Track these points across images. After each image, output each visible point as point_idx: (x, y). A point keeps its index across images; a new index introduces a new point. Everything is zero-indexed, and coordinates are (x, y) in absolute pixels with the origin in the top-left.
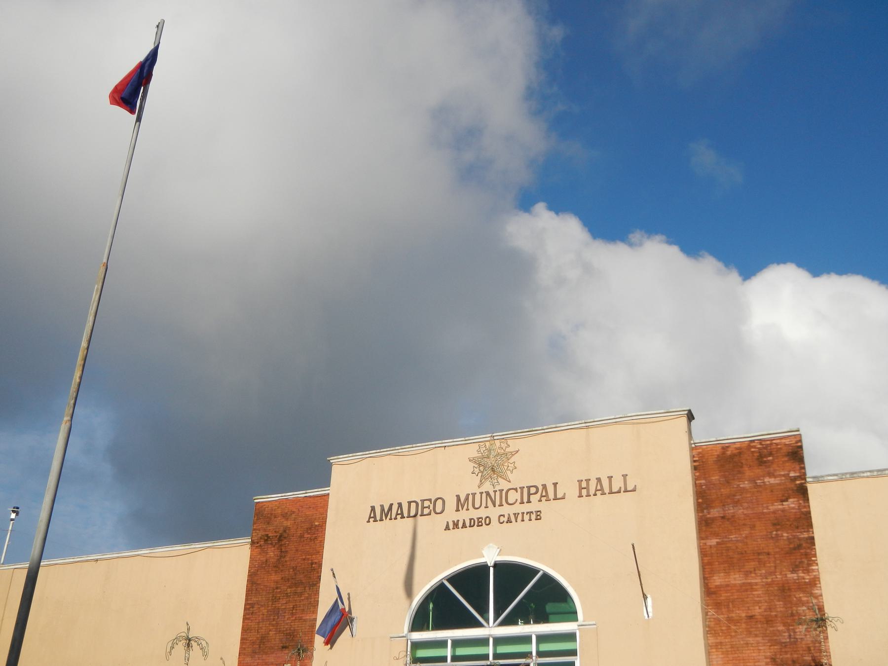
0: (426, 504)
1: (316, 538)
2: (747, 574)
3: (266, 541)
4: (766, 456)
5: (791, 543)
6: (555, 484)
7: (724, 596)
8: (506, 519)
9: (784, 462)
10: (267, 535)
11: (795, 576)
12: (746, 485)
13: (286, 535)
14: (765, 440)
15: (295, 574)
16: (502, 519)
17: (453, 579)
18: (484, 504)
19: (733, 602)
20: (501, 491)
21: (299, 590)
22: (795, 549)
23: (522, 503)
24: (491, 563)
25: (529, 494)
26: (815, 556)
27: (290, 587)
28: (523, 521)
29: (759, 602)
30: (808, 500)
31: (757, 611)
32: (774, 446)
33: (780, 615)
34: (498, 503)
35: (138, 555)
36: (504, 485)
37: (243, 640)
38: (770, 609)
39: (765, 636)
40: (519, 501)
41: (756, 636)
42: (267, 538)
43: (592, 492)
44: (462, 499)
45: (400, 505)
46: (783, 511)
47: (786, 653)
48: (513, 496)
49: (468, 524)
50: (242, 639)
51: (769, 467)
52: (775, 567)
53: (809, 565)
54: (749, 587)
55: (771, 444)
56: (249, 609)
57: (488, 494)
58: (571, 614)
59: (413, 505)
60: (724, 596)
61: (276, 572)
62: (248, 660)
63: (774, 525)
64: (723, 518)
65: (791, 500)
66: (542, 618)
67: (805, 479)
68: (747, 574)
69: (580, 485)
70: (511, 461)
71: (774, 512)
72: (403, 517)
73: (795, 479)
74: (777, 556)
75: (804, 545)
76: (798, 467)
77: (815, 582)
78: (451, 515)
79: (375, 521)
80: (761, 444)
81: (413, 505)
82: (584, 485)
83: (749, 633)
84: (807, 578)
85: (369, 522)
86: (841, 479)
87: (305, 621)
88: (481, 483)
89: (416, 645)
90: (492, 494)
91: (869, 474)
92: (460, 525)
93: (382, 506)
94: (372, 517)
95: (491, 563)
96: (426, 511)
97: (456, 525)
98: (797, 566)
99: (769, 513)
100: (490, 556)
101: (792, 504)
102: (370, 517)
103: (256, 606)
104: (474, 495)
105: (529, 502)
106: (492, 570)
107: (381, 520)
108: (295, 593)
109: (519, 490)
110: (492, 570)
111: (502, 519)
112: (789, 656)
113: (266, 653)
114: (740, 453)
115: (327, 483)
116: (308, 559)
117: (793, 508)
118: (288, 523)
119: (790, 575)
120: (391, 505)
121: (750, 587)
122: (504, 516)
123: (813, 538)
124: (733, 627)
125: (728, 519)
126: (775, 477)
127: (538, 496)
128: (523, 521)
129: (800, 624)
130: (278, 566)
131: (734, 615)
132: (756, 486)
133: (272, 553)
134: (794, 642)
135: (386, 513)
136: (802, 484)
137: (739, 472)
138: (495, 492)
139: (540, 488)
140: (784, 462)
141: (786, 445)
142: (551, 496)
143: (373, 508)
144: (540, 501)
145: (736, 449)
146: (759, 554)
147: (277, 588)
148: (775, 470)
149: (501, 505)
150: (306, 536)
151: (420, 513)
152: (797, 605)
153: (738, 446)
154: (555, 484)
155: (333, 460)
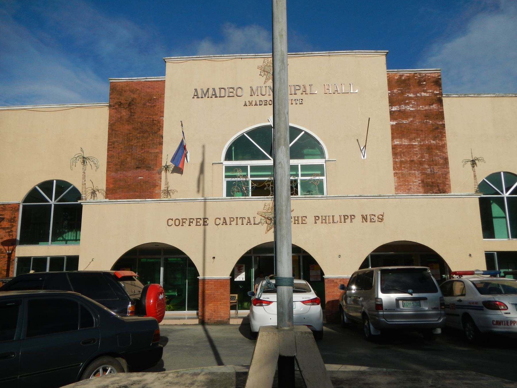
0: (231, 90)
1: (155, 106)
2: (411, 140)
3: (120, 105)
5: (433, 126)
7: (399, 150)
9: (432, 86)
10: (120, 102)
12: (411, 95)
13: (134, 103)
15: (142, 126)
17: (251, 133)
18: (268, 94)
19: (403, 153)
21: (145, 135)
26: (445, 133)
27: (139, 133)
29: (417, 154)
31: (415, 158)
37: (108, 162)
38: (422, 157)
39: (418, 170)
41: (414, 170)
42: (120, 104)
44: (254, 89)
45: (214, 89)
46: (430, 110)
47: (429, 179)
49: (258, 103)
50: (108, 162)
51: (424, 87)
52: (425, 137)
53: (442, 137)
56: (111, 145)
58: (322, 155)
60: (399, 150)
61: (128, 124)
62: (113, 174)
63: (425, 116)
66: (302, 157)
67: (442, 95)
68: (411, 140)
71: (426, 110)
72: (216, 97)
73: (437, 94)
76: (438, 89)
77: (444, 146)
78: (246, 97)
83: (411, 169)
84: (441, 143)
86: (459, 97)
87: (151, 153)
88: (265, 82)
89: (228, 169)
91: (473, 95)
92: (254, 103)
94: (196, 96)
96: (231, 94)
97: (251, 104)
98: (436, 138)
99: (423, 111)
101: (434, 106)
103: (116, 144)
108: (143, 137)
112: (430, 180)
113: (126, 171)
114: (409, 79)
116: (150, 118)
117: (435, 109)
118: (135, 96)
119: (432, 142)
120: (208, 89)
121: (413, 146)
123: (444, 124)
125: (402, 112)
126: (427, 93)
127: (300, 91)
129: (436, 165)
130: (129, 121)
132: (417, 97)
133: (125, 113)
134: (433, 174)
137: (408, 89)
139: (302, 87)
140: (432, 86)
142: (308, 91)
143: (196, 90)
145: (407, 76)
146: (417, 130)
147: (130, 134)
148: (427, 89)
150: (148, 104)
152: (435, 156)
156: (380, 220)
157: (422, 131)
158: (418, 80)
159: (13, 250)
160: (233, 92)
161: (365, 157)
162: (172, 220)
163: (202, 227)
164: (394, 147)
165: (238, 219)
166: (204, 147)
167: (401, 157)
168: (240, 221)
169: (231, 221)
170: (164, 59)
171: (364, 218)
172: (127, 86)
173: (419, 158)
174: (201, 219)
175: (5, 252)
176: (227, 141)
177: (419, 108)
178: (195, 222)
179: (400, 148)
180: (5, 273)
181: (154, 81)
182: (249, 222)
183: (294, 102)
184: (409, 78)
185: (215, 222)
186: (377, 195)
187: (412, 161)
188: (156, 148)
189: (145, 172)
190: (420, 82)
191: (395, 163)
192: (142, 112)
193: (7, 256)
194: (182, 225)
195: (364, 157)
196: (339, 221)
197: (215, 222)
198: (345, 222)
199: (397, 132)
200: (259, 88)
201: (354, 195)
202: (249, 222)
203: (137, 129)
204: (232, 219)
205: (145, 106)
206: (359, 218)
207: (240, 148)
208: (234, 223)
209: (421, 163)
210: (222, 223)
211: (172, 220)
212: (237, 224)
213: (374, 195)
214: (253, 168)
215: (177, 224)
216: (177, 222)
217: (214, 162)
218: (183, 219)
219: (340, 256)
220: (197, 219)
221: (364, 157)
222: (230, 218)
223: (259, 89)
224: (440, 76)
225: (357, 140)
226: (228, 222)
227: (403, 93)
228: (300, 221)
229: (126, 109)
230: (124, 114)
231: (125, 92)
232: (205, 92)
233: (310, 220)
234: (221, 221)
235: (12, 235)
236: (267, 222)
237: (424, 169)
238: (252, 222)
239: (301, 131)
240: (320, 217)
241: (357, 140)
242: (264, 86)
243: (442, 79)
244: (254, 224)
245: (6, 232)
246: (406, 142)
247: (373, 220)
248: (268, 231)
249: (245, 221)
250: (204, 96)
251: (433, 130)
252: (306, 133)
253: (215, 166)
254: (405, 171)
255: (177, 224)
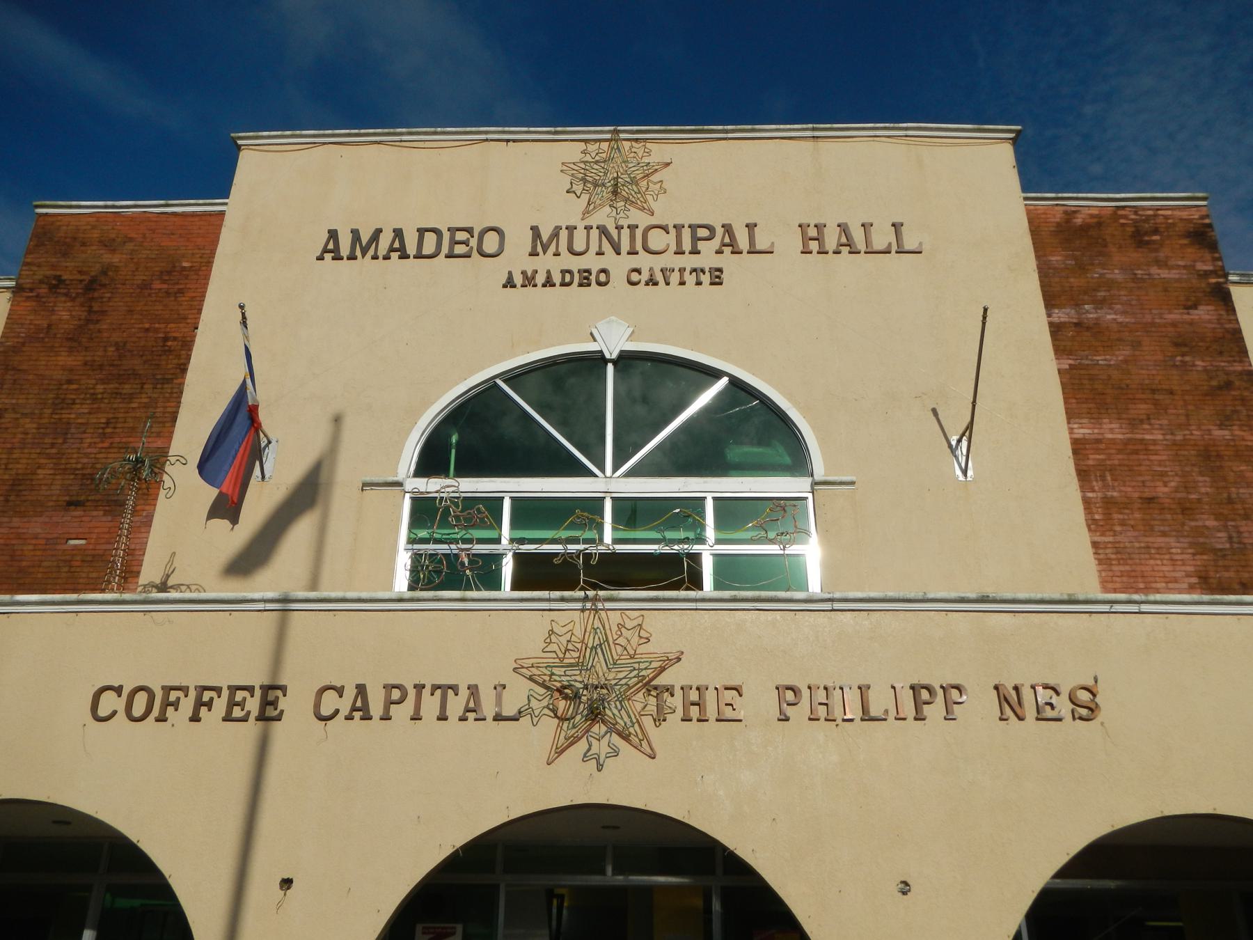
1: (181, 291)
2: (1134, 424)
4: (1146, 233)
5: (1211, 378)
6: (751, 227)
7: (1093, 459)
8: (645, 276)
10: (58, 278)
11: (1226, 433)
12: (1117, 275)
13: (105, 281)
14: (1144, 208)
15: (120, 357)
16: (635, 277)
20: (633, 228)
21: (127, 388)
22: (1220, 388)
23: (680, 252)
24: (612, 353)
25: (695, 239)
27: (103, 381)
28: (682, 283)
30: (1234, 310)
31: (1162, 490)
32: (1160, 220)
33: (1206, 499)
34: (625, 246)
36: (643, 220)
40: (673, 247)
41: (1164, 534)
42: (56, 284)
43: (831, 244)
44: (545, 237)
46: (1191, 323)
47: (1227, 568)
48: (657, 240)
49: (557, 278)
51: (1156, 250)
52: (1187, 416)
54: (1140, 447)
55: (1155, 216)
57: (603, 230)
58: (798, 462)
59: (430, 239)
61: (71, 350)
63: (1176, 345)
64: (1076, 324)
65: (1201, 307)
67: (1226, 275)
68: (1134, 424)
69: (804, 234)
70: (655, 178)
72: (404, 256)
73: (1206, 274)
74: (1187, 397)
75: (1237, 383)
78: (517, 258)
79: (338, 258)
80: (1136, 213)
81: (430, 239)
82: (813, 232)
83: (1149, 529)
85: (320, 258)
88: (586, 213)
90: (614, 233)
92: (540, 279)
93: (356, 234)
94: (331, 249)
95: (612, 353)
96: (459, 249)
97: (529, 280)
98: (1228, 418)
99: (1165, 326)
100: (614, 339)
101: (1205, 313)
102: (325, 251)
104: (571, 229)
105: (695, 251)
106: (610, 367)
107: (352, 257)
108: (116, 394)
109: (673, 231)
110: (610, 367)
111: (635, 277)
114: (1099, 224)
115: (222, 188)
116: (157, 331)
117: (1210, 321)
118: (116, 259)
119: (1217, 433)
120: (379, 231)
122: (638, 271)
124: (1116, 516)
125: (1088, 329)
126: (1170, 268)
127: (715, 243)
128: (682, 283)
130: (74, 340)
131: (1115, 494)
132: (1135, 279)
135: (364, 246)
136: (1218, 283)
138: (619, 228)
139: (720, 231)
140: (1183, 246)
141: (1181, 219)
142: (743, 243)
143: (333, 234)
144: (719, 252)
145: (1092, 216)
146: (1153, 391)
147: (69, 382)
149: (633, 252)
150: (157, 285)
151: (445, 249)
153: (1095, 212)
154: (751, 227)
155: (244, 139)
156: (1084, 712)
157: (1171, 392)
158: (1130, 229)
160: (463, 243)
161: (970, 473)
162: (118, 690)
163: (251, 729)
164: (1079, 448)
165: (426, 692)
166: (337, 420)
167: (1106, 486)
168: (431, 705)
169: (389, 703)
170: (234, 140)
171: (1009, 702)
172: (94, 227)
173: (1176, 490)
174: (250, 689)
176: (427, 405)
177: (1148, 318)
178: (220, 705)
179: (1098, 451)
181: (194, 214)
182: (472, 710)
183: (690, 279)
184: (1098, 223)
185: (317, 705)
186: (1057, 596)
187: (1150, 500)
188: (159, 435)
189: (98, 521)
190: (1143, 233)
191: (1087, 502)
192: (130, 312)
194: (162, 719)
195: (965, 472)
196: (893, 713)
197: (317, 705)
198: (919, 718)
199: (1084, 392)
200: (564, 234)
201: (953, 595)
202: (472, 710)
203: (101, 367)
204: (395, 693)
205: (146, 292)
206: (979, 705)
207: (477, 434)
208: (402, 712)
209: (1186, 509)
210: (345, 711)
211: (118, 690)
212: (416, 717)
213: (1046, 596)
214: (531, 512)
215: (138, 710)
216: (140, 701)
217: (368, 479)
218: (167, 690)
219: (905, 888)
220: (234, 689)
221: (965, 472)
222: (389, 688)
223: (564, 234)
224: (1207, 216)
225: (934, 411)
226: (376, 708)
227: (1082, 268)
228: (711, 711)
229: (73, 300)
230: (65, 315)
231: (84, 244)
232: (365, 240)
233: (759, 702)
234: (345, 705)
236: (554, 711)
237: (1199, 532)
238: (489, 709)
239: (715, 374)
240: (806, 693)
241: (934, 411)
242: (581, 226)
243: (1217, 226)
244: (498, 718)
246: (1113, 430)
247: (1049, 713)
248: (560, 752)
249: (456, 705)
250: (358, 253)
251: (1213, 392)
252: (735, 383)
253: (371, 494)
254: (1127, 538)
255: (138, 710)
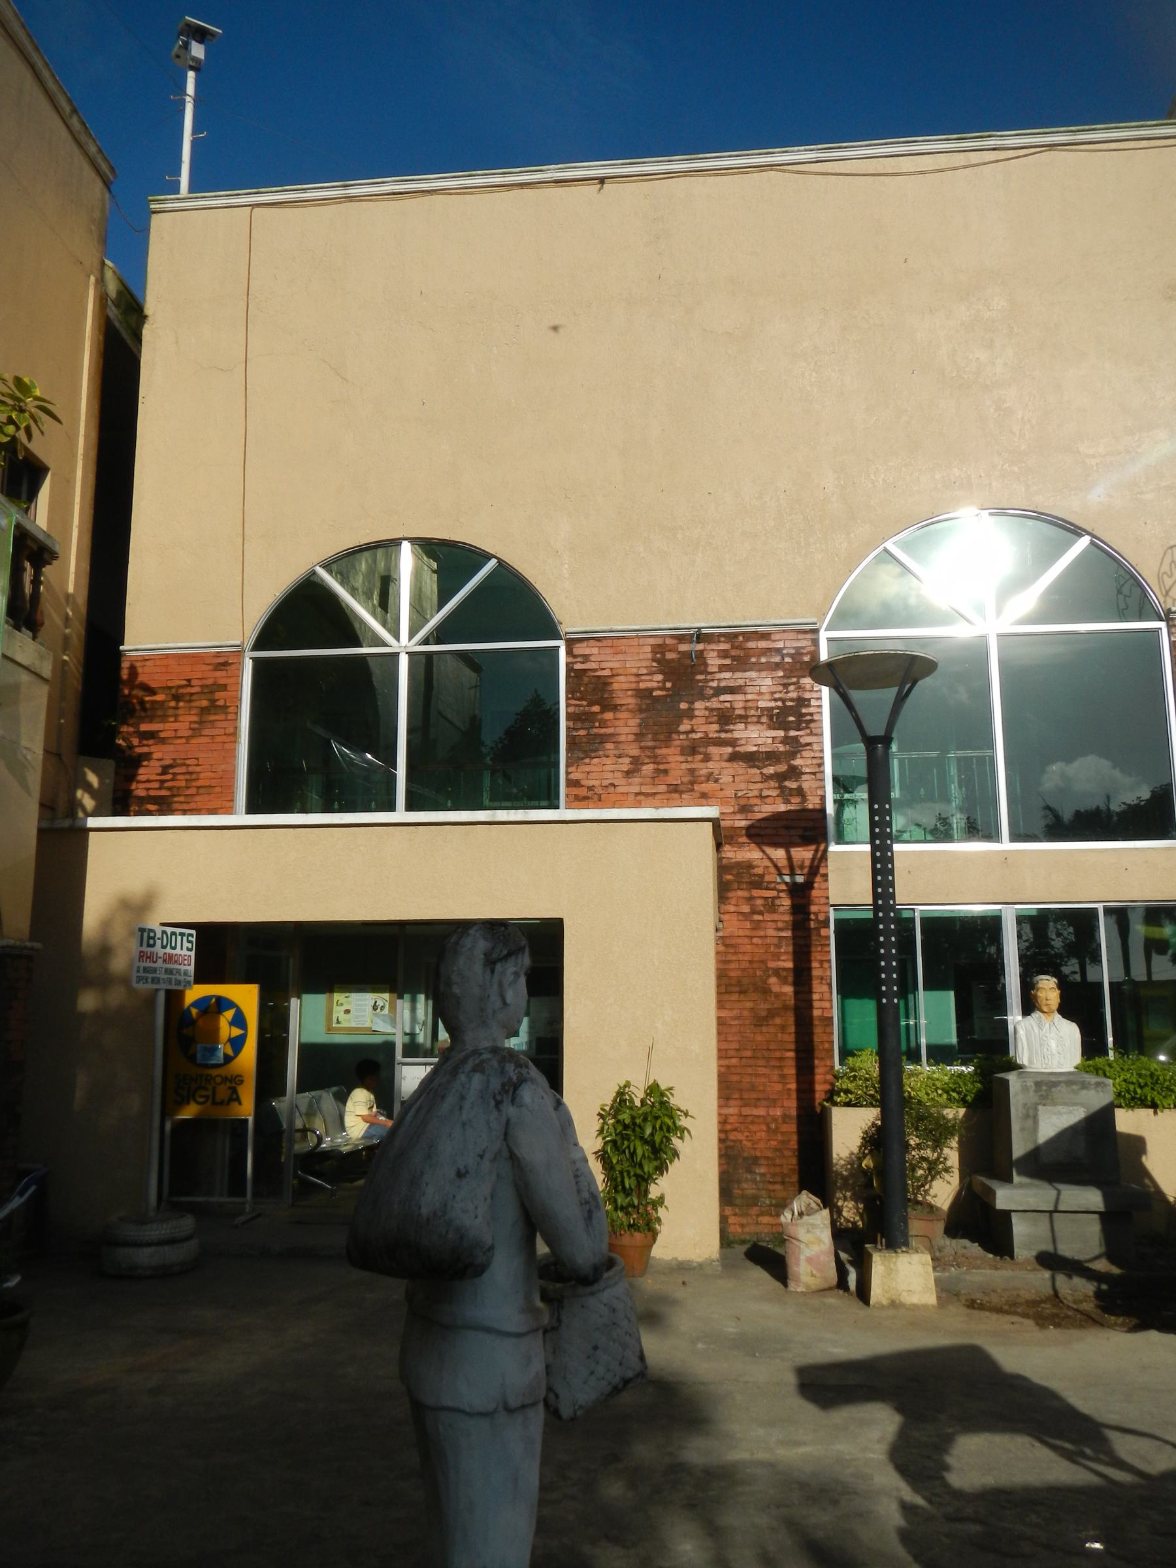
35: (770, 167)
159: (816, 869)
175: (772, 877)
180: (789, 989)
193: (786, 902)
235: (800, 792)
245: (766, 778)
